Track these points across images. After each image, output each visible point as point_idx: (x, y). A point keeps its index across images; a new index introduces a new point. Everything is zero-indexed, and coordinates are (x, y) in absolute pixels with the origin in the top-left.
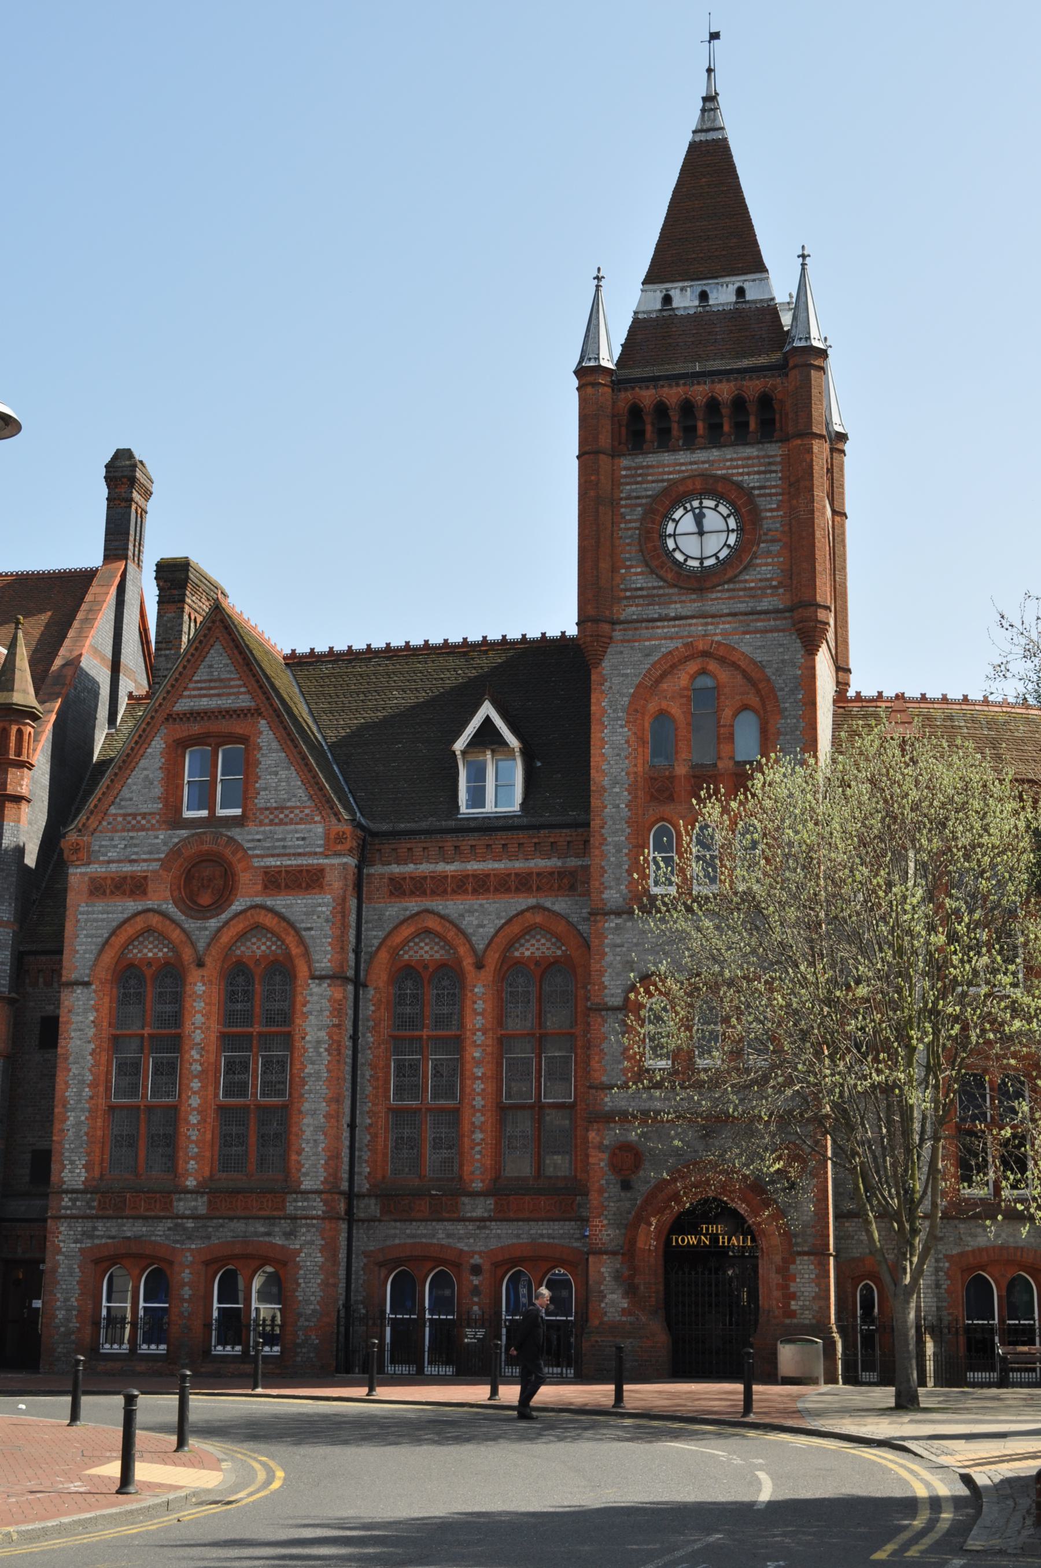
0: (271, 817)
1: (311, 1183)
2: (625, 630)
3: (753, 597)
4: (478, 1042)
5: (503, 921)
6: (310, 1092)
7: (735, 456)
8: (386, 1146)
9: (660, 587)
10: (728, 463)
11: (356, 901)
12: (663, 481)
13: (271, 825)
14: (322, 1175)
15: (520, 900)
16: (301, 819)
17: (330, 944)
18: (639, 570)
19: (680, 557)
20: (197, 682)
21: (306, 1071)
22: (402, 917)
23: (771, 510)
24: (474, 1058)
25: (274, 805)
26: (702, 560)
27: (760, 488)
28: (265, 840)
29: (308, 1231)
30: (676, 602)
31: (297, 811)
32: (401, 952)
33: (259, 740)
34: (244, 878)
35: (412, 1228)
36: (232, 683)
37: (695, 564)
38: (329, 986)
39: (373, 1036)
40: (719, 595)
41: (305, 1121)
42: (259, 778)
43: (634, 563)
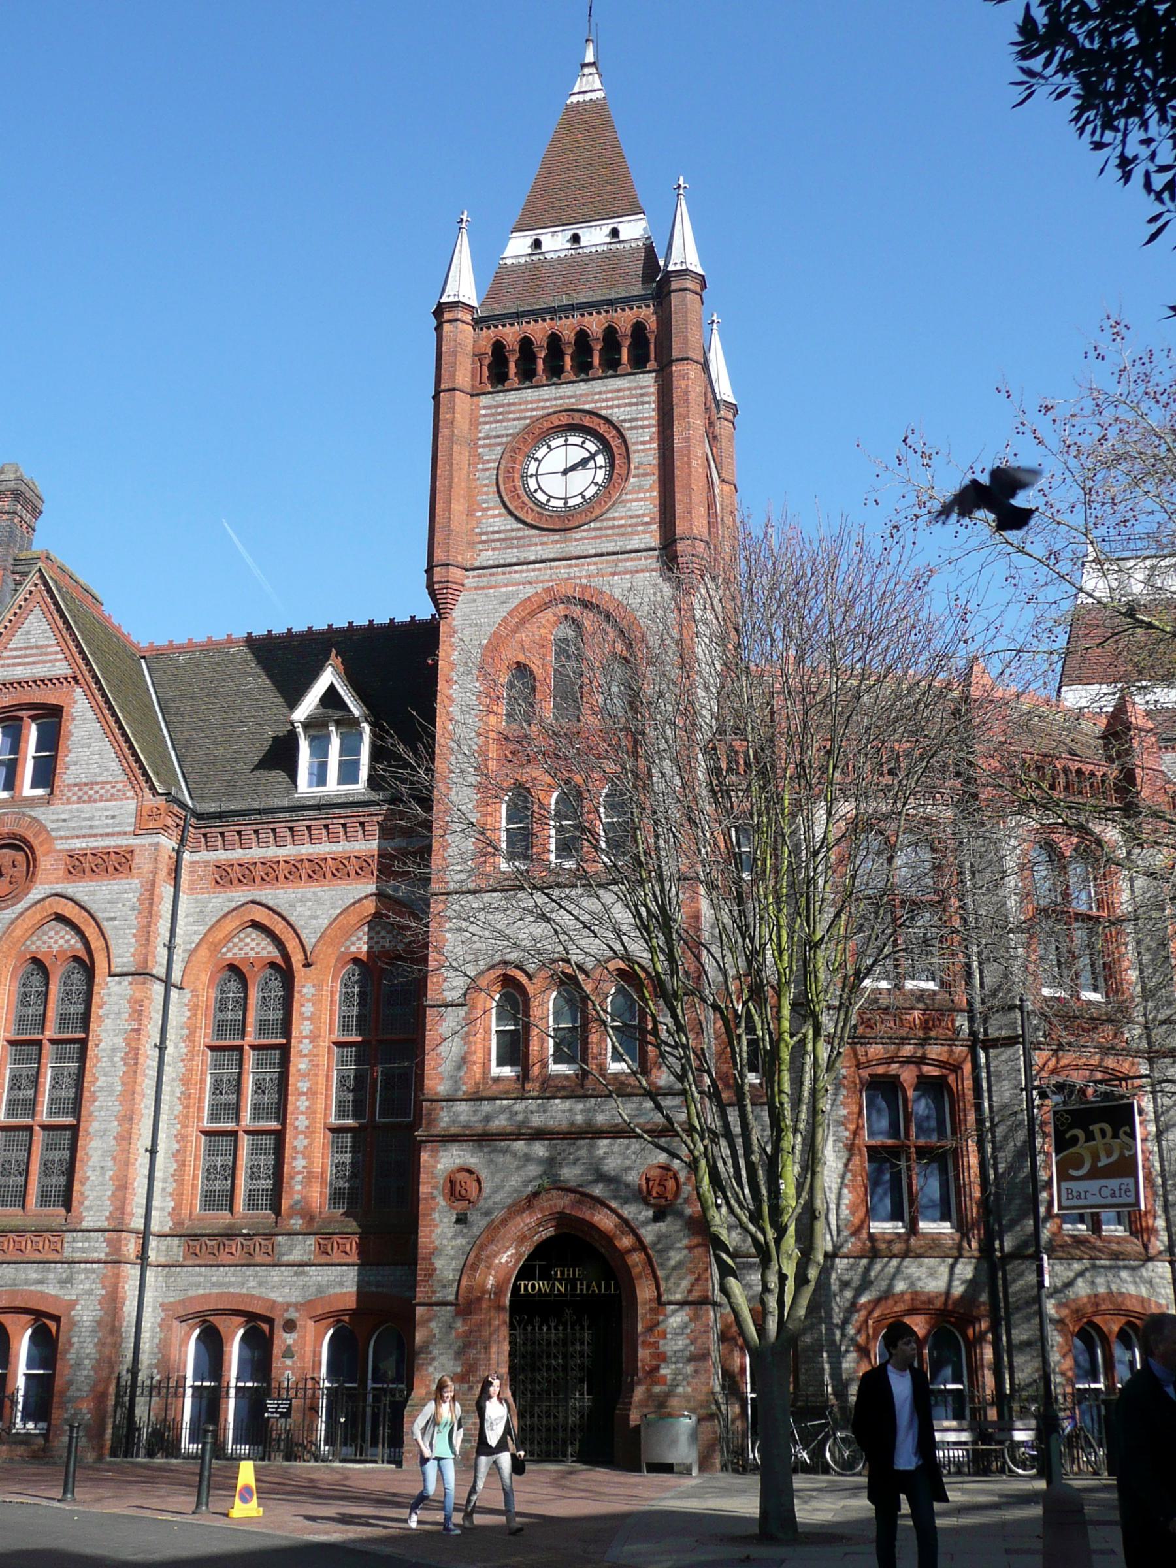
0: (80, 793)
1: (95, 1219)
2: (479, 576)
3: (623, 535)
4: (305, 1052)
5: (339, 911)
6: (101, 1109)
7: (604, 389)
8: (195, 1177)
9: (519, 529)
10: (597, 397)
11: (172, 889)
12: (525, 418)
13: (79, 803)
14: (108, 1208)
15: (359, 886)
16: (112, 795)
17: (134, 935)
18: (497, 512)
19: (542, 498)
20: (11, 650)
21: (99, 1084)
22: (226, 910)
23: (644, 443)
24: (299, 1070)
25: (84, 780)
26: (566, 499)
27: (630, 421)
28: (70, 820)
29: (87, 1278)
30: (536, 545)
31: (108, 787)
32: (224, 950)
33: (73, 710)
34: (45, 863)
35: (217, 1275)
36: (49, 650)
37: (560, 503)
38: (131, 984)
39: (187, 1046)
40: (585, 534)
41: (93, 1144)
42: (70, 751)
43: (491, 505)
